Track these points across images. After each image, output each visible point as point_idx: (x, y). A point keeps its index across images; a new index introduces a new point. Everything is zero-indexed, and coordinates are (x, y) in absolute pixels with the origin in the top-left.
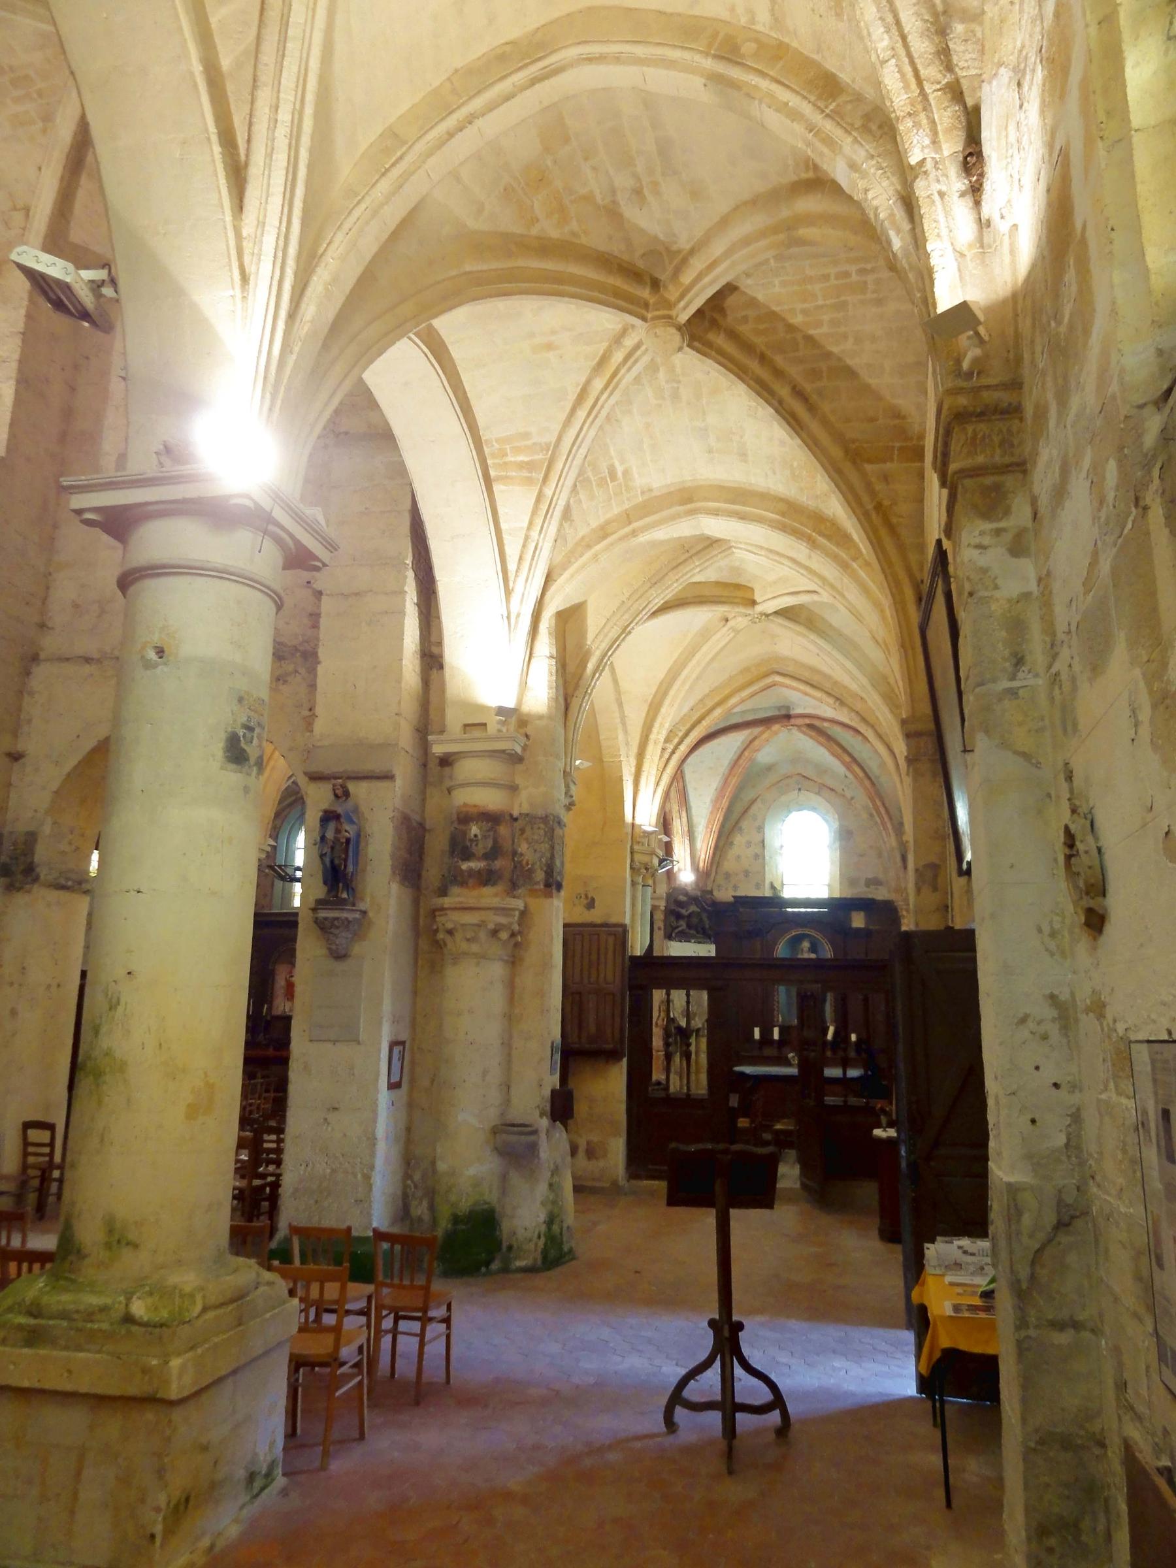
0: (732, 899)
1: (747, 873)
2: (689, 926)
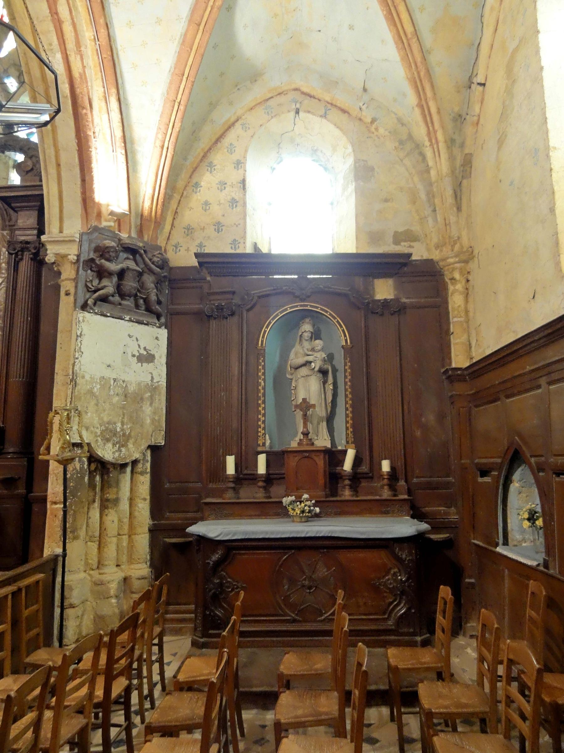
0: (194, 262)
1: (218, 227)
2: (120, 292)
